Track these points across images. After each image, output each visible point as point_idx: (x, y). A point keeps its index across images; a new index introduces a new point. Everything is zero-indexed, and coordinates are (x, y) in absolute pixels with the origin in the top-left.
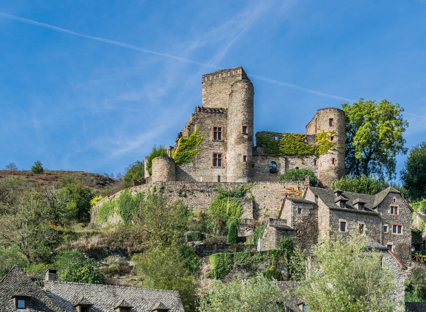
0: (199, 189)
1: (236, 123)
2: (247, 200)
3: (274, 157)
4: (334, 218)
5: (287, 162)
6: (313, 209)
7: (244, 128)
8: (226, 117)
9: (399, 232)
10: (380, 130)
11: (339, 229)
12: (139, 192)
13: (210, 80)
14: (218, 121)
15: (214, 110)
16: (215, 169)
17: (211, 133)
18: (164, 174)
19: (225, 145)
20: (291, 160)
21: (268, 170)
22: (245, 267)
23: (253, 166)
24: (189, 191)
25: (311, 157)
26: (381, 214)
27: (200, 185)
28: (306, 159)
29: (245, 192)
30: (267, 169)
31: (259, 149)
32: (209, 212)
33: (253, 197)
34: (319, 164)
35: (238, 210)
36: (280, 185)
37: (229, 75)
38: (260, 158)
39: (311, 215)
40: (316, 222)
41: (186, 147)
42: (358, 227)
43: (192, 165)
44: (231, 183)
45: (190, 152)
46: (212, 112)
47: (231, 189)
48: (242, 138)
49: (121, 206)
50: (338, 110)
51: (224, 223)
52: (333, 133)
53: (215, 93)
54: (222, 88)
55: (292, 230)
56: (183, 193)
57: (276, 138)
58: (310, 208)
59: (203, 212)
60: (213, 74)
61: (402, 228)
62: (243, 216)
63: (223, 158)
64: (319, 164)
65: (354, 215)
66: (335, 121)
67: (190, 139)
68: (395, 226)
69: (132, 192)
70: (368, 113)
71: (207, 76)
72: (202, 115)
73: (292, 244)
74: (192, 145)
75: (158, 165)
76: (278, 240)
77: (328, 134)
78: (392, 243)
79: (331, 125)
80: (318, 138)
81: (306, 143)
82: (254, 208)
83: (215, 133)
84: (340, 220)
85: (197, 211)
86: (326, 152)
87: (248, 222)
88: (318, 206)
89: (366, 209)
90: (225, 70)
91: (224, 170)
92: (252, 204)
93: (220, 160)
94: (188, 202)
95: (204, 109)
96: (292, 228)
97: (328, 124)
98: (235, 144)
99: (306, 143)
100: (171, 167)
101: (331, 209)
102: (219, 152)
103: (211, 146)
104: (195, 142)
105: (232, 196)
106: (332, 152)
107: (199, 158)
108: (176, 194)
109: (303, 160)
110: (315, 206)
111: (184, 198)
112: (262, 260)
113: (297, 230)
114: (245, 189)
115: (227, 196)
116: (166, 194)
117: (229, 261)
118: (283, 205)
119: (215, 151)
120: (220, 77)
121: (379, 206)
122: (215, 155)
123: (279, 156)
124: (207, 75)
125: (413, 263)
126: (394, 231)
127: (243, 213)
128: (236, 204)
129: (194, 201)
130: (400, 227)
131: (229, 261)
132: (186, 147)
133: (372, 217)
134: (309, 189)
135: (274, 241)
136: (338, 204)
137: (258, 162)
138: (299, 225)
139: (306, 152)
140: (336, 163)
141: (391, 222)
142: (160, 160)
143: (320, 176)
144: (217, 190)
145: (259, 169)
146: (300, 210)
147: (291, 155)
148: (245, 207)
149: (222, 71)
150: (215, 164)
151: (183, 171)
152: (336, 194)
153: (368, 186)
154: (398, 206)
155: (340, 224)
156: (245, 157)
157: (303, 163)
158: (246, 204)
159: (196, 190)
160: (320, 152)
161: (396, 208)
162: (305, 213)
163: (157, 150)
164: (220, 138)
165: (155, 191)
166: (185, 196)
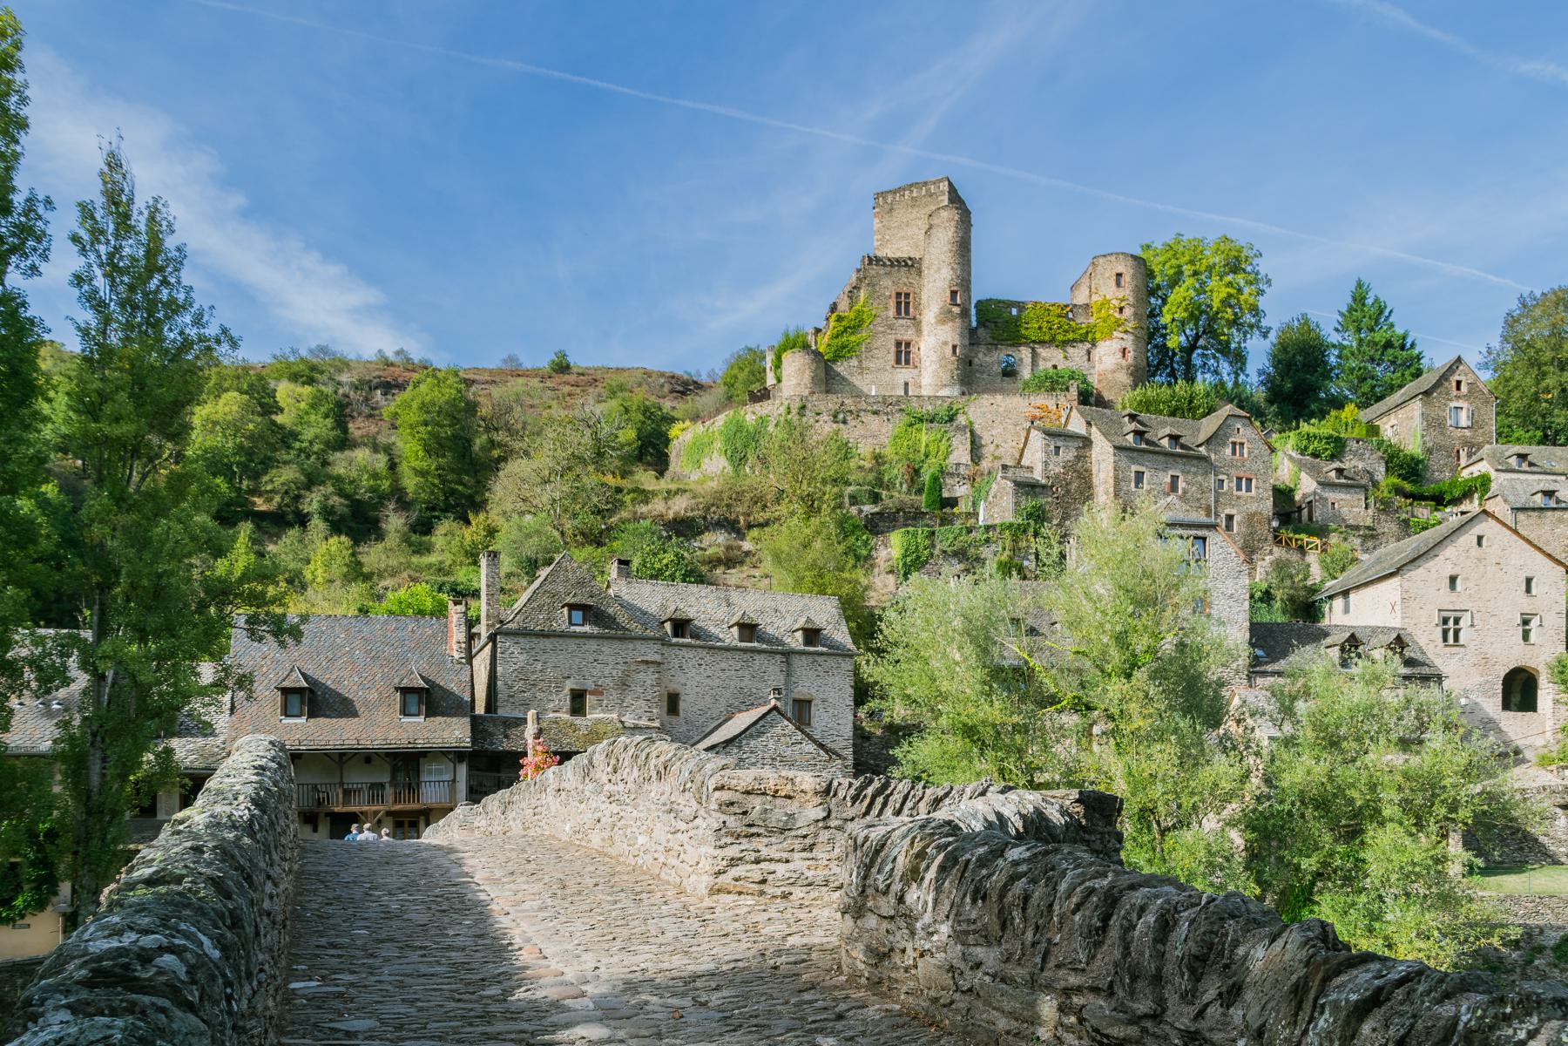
1: (938, 284)
2: (958, 428)
3: (1012, 345)
4: (1123, 464)
5: (1035, 355)
6: (1084, 448)
7: (954, 293)
8: (920, 272)
9: (1249, 489)
10: (1215, 294)
11: (1133, 484)
14: (903, 279)
15: (897, 261)
17: (892, 304)
19: (917, 324)
20: (1043, 352)
21: (1000, 370)
22: (955, 554)
23: (970, 363)
24: (851, 412)
25: (1080, 345)
26: (1213, 456)
27: (871, 400)
28: (1070, 350)
29: (956, 414)
30: (997, 369)
31: (981, 331)
32: (888, 452)
33: (971, 423)
35: (942, 448)
36: (1021, 399)
38: (983, 349)
39: (1078, 458)
40: (1089, 471)
42: (1168, 480)
43: (856, 364)
44: (929, 397)
45: (853, 338)
46: (892, 265)
47: (930, 408)
48: (950, 312)
49: (727, 440)
50: (1132, 256)
51: (917, 472)
52: (1122, 301)
53: (899, 227)
55: (1044, 487)
56: (841, 416)
57: (1014, 311)
58: (1076, 445)
59: (877, 451)
60: (894, 192)
61: (1254, 481)
62: (953, 459)
65: (1161, 458)
66: (1127, 278)
67: (852, 315)
68: (1239, 479)
70: (1192, 262)
71: (883, 194)
73: (1043, 512)
74: (855, 328)
76: (1017, 504)
77: (1114, 302)
78: (1233, 512)
79: (1118, 284)
80: (1094, 310)
81: (1070, 320)
82: (973, 442)
83: (899, 304)
84: (1134, 468)
85: (865, 449)
86: (1109, 336)
87: (962, 470)
88: (1091, 442)
89: (1183, 447)
91: (916, 371)
92: (968, 435)
93: (908, 353)
94: (850, 433)
95: (878, 260)
96: (1044, 482)
97: (1114, 283)
99: (1070, 320)
100: (817, 368)
101: (1116, 448)
103: (891, 327)
104: (862, 321)
105: (932, 422)
107: (869, 350)
108: (826, 418)
110: (1087, 442)
111: (842, 426)
112: (987, 541)
113: (1052, 486)
115: (921, 420)
116: (809, 418)
117: (927, 542)
118: (1027, 439)
119: (899, 337)
121: (1208, 442)
122: (898, 344)
123: (1020, 345)
125: (1275, 549)
126: (1239, 488)
127: (951, 452)
128: (939, 436)
129: (860, 430)
130: (1249, 480)
131: (927, 542)
133: (1195, 462)
134: (1074, 410)
135: (1011, 506)
136: (1130, 437)
137: (980, 355)
138: (1057, 476)
139: (1071, 336)
140: (1130, 356)
141: (1233, 472)
142: (797, 355)
143: (1099, 381)
145: (981, 369)
146: (1057, 448)
147: (1042, 343)
148: (955, 442)
149: (911, 185)
150: (898, 361)
151: (839, 375)
152: (1127, 419)
153: (1191, 402)
154: (1245, 440)
155: (1133, 475)
156: (954, 347)
157: (1066, 357)
158: (958, 435)
160: (1098, 335)
161: (1242, 444)
162: (1068, 454)
163: (792, 336)
164: (907, 312)
166: (845, 422)
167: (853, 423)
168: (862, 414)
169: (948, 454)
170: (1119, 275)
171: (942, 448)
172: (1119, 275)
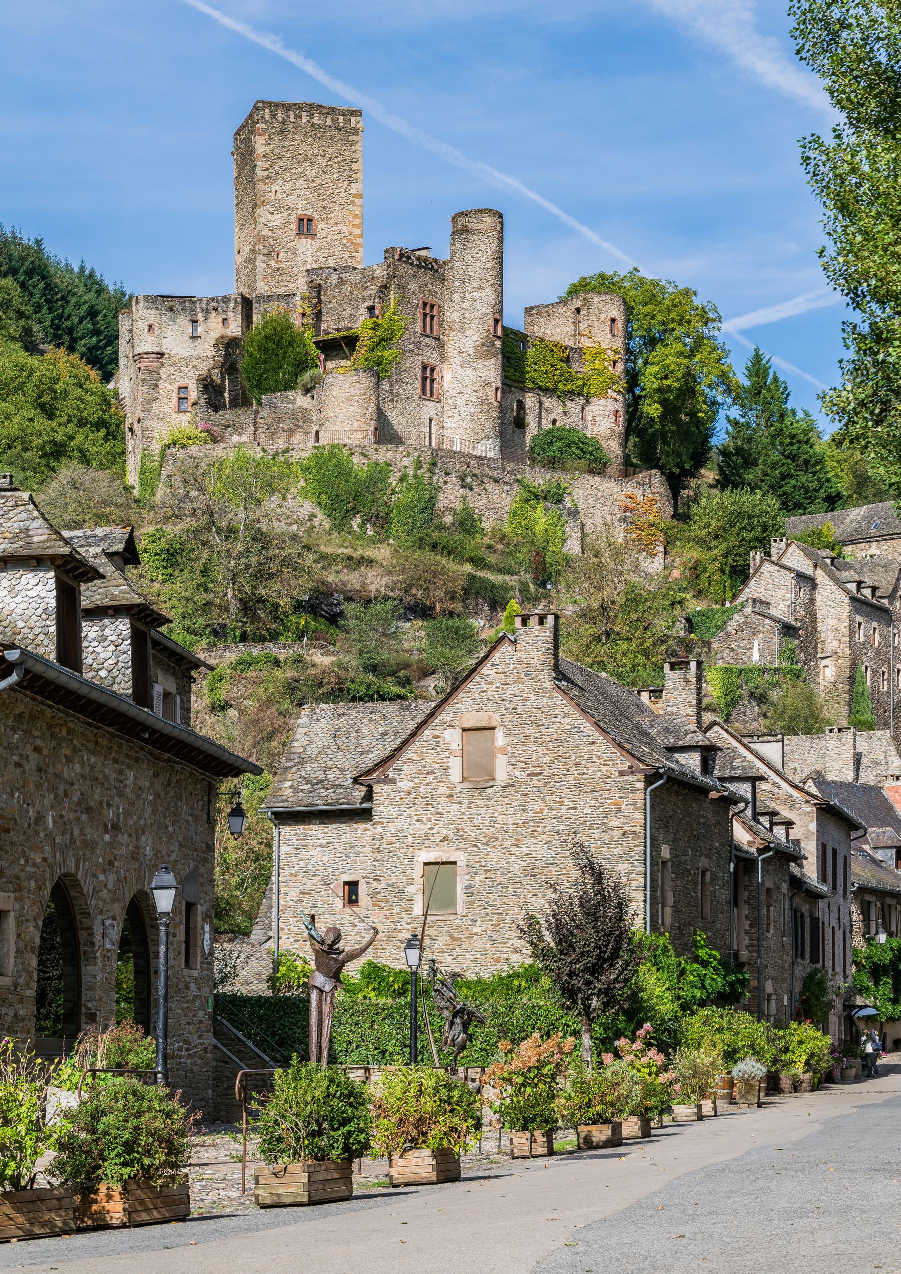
0: (491, 474)
12: (374, 459)
13: (280, 119)
16: (425, 402)
18: (371, 409)
32: (507, 529)
34: (590, 418)
35: (559, 533)
37: (329, 122)
41: (379, 344)
47: (541, 482)
48: (493, 345)
56: (468, 480)
60: (288, 107)
63: (439, 379)
64: (590, 418)
69: (353, 454)
72: (404, 269)
74: (385, 341)
75: (358, 386)
77: (608, 352)
83: (425, 315)
90: (319, 106)
91: (439, 406)
93: (433, 381)
94: (476, 502)
98: (476, 354)
102: (431, 362)
106: (614, 395)
108: (454, 480)
109: (564, 405)
111: (468, 491)
114: (563, 485)
116: (439, 479)
120: (304, 121)
122: (425, 368)
124: (270, 103)
132: (379, 344)
139: (569, 387)
144: (518, 480)
147: (546, 390)
150: (424, 393)
156: (497, 389)
157: (565, 413)
165: (420, 468)
166: (471, 489)
167: (477, 490)
168: (485, 479)
169: (564, 541)
170: (613, 321)
171: (559, 533)
172: (613, 321)
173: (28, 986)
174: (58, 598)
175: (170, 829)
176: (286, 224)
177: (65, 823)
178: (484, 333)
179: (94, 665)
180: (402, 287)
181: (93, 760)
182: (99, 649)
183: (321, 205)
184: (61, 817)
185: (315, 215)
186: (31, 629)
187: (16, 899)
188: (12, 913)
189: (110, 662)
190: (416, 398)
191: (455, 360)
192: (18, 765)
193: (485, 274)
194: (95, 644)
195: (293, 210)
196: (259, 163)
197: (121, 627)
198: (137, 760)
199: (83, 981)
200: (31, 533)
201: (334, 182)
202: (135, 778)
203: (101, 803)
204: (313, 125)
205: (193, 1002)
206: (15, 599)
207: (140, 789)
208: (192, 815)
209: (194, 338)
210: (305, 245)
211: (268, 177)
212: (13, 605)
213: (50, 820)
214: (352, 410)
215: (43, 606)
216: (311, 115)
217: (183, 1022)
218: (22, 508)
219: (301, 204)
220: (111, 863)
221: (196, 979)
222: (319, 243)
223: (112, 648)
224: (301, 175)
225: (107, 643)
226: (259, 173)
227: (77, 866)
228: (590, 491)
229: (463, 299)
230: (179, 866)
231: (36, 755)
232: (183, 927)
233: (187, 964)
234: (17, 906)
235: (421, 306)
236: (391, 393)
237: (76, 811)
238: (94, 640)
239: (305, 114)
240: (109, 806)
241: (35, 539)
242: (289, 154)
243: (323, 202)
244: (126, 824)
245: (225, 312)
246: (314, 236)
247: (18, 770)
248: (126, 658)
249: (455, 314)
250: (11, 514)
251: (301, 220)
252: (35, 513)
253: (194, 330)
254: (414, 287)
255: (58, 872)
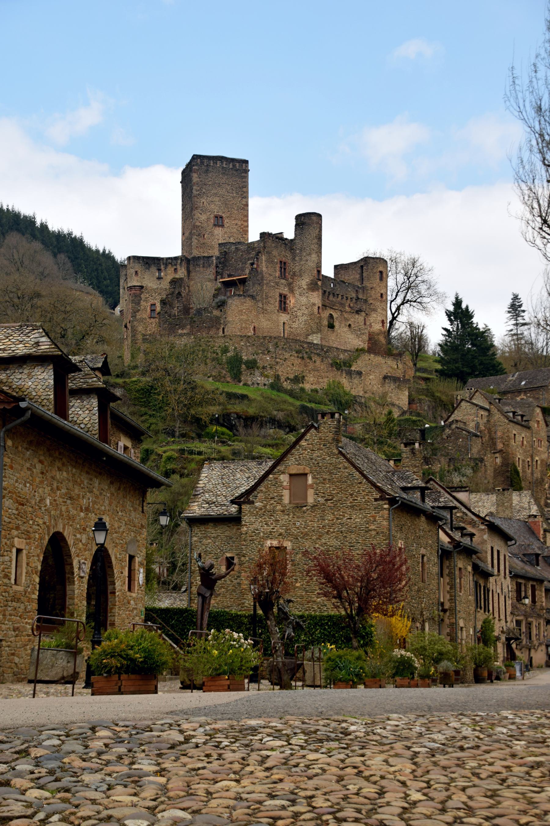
16: (281, 314)
19: (290, 286)
37: (231, 166)
48: (317, 284)
54: (223, 181)
63: (288, 302)
83: (281, 268)
93: (285, 303)
98: (308, 289)
102: (284, 292)
122: (281, 295)
156: (319, 307)
159: (315, 354)
173: (34, 593)
174: (55, 380)
175: (120, 513)
176: (208, 219)
177: (57, 504)
178: (312, 278)
179: (78, 421)
180: (269, 253)
181: (74, 470)
182: (80, 412)
183: (226, 210)
184: (55, 500)
185: (223, 215)
186: (40, 396)
187: (27, 543)
188: (24, 551)
189: (86, 419)
190: (276, 311)
191: (297, 292)
192: (28, 469)
193: (312, 247)
194: (79, 409)
195: (212, 212)
196: (194, 187)
197: (92, 400)
198: (100, 474)
199: (68, 594)
200: (40, 344)
201: (234, 198)
202: (99, 484)
203: (79, 495)
204: (223, 168)
205: (132, 611)
206: (32, 380)
207: (102, 489)
208: (132, 506)
209: (159, 278)
210: (218, 231)
211: (199, 195)
212: (30, 383)
213: (48, 502)
214: (241, 317)
215: (47, 384)
216: (222, 163)
217: (127, 621)
218: (36, 331)
219: (216, 208)
220: (84, 529)
221: (134, 598)
222: (225, 230)
223: (87, 412)
224: (216, 194)
225: (85, 409)
226: (195, 192)
227: (64, 528)
228: (367, 362)
229: (301, 260)
230: (125, 534)
231: (40, 465)
232: (127, 569)
233: (130, 589)
234: (27, 547)
235: (279, 263)
236: (263, 308)
237: (64, 498)
238: (78, 407)
239: (218, 162)
240: (83, 497)
241: (42, 347)
242: (210, 183)
243: (228, 208)
244: (94, 508)
245: (176, 265)
246: (222, 226)
247: (29, 473)
248: (96, 417)
249: (297, 267)
250: (29, 335)
251: (216, 217)
252: (44, 334)
253: (160, 274)
254: (275, 253)
255: (52, 531)
